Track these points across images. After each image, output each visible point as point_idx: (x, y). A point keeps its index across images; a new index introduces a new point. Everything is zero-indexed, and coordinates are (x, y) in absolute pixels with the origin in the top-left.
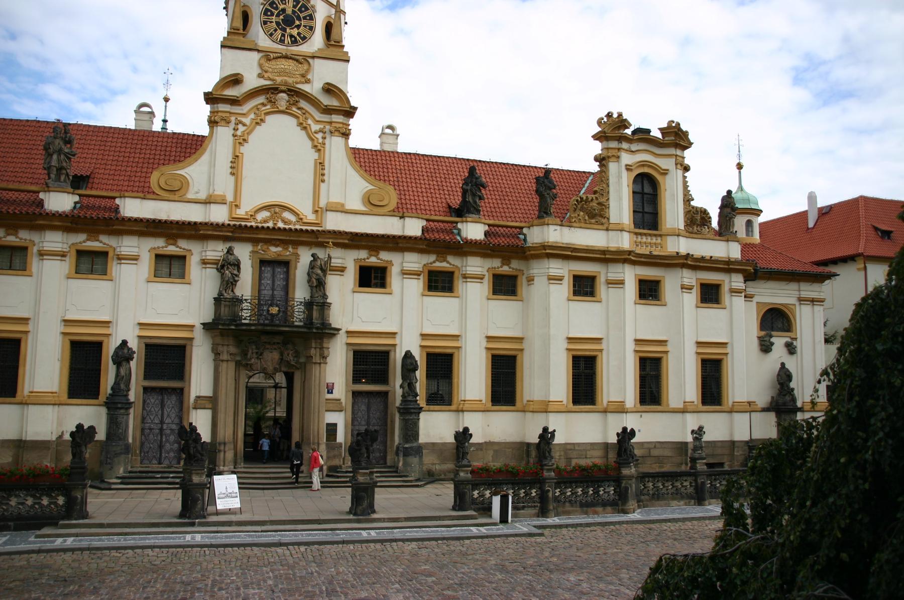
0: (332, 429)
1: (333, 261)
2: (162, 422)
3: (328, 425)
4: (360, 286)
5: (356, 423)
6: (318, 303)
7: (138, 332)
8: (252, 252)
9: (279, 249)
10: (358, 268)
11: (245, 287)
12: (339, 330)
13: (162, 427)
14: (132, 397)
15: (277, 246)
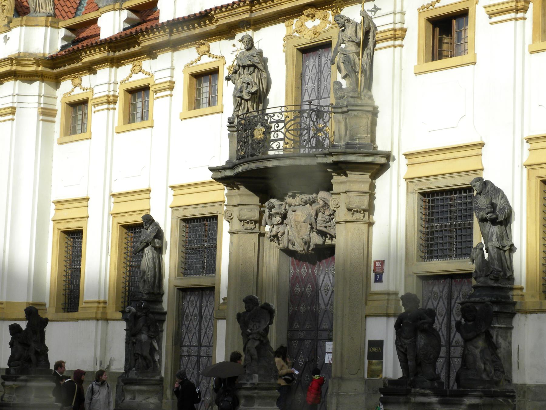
0: (376, 349)
1: (377, 22)
2: (200, 346)
3: (372, 343)
4: (426, 61)
5: (296, 326)
6: (357, 104)
7: (171, 201)
8: (288, 37)
9: (317, 22)
10: (423, 22)
11: (278, 98)
12: (388, 156)
13: (199, 352)
14: (165, 306)
15: (313, 16)
